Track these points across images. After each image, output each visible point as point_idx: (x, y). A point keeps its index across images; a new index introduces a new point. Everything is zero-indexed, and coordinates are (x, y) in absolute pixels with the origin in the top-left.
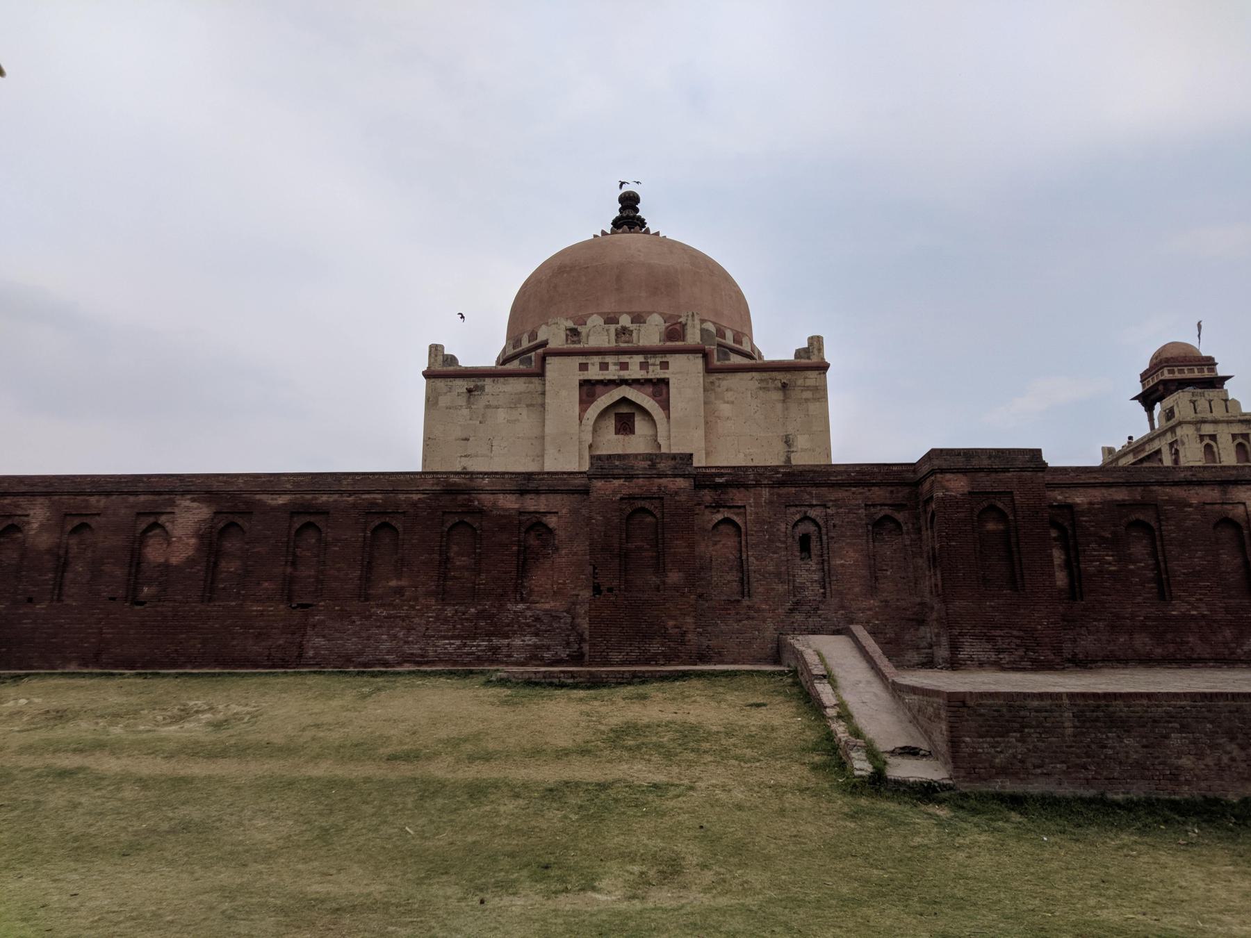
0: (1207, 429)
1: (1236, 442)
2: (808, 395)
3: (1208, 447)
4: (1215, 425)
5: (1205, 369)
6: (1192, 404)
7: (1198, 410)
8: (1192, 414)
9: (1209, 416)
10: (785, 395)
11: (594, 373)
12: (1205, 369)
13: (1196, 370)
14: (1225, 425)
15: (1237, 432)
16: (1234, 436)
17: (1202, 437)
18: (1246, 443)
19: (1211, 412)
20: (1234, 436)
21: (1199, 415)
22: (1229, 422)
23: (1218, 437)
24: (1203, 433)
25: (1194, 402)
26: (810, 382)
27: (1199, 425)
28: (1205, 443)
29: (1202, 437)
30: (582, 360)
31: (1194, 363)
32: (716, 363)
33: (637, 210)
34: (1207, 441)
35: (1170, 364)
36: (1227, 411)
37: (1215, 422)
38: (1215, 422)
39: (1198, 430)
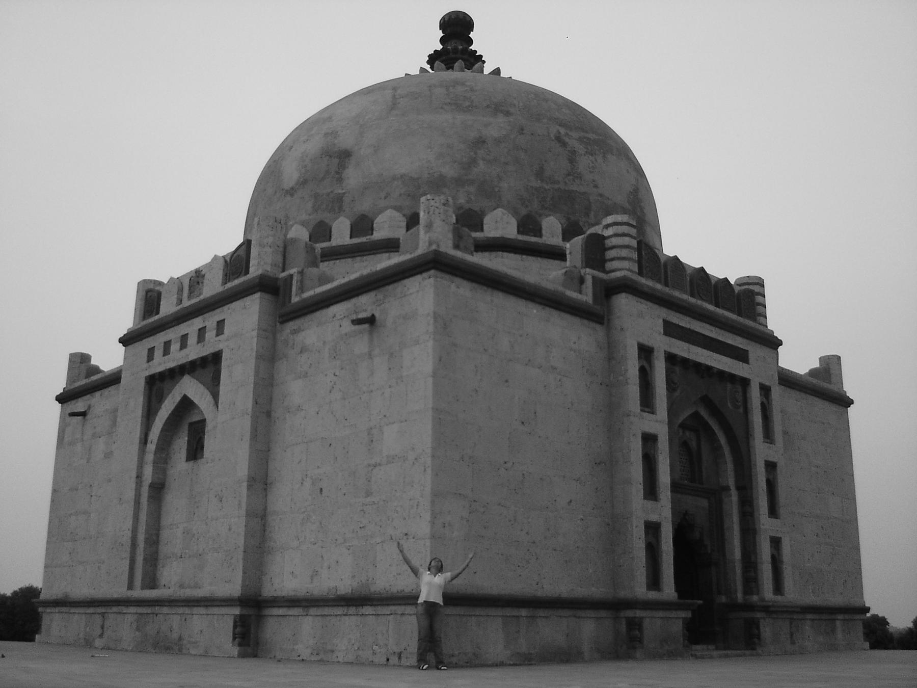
11: (160, 364)
33: (471, 42)
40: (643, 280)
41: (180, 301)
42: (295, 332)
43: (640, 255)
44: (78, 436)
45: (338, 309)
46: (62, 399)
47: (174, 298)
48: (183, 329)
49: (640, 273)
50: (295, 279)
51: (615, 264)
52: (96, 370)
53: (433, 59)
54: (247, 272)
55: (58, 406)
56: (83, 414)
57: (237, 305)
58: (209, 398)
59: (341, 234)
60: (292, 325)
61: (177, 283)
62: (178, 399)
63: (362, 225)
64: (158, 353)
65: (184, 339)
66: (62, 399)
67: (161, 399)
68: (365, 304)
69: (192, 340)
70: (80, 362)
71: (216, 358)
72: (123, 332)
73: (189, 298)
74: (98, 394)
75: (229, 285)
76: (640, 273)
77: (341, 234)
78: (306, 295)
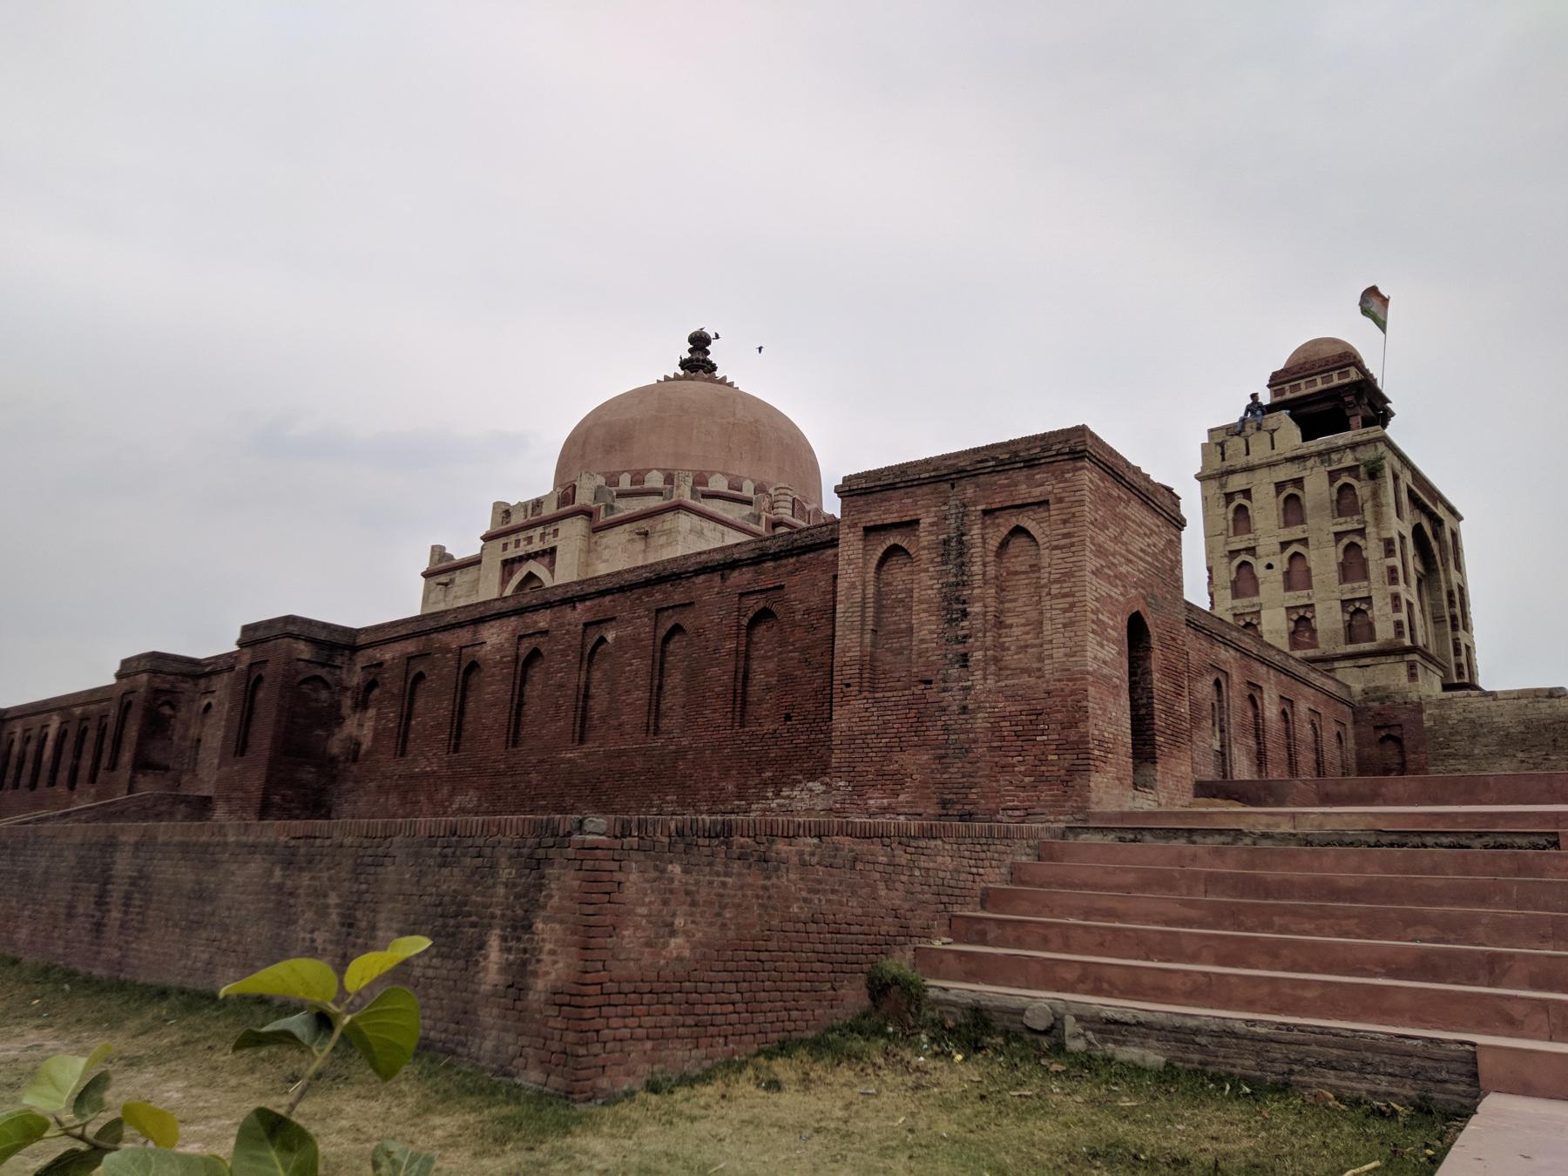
0: (1237, 483)
2: (663, 540)
4: (1250, 474)
5: (1335, 375)
6: (1219, 448)
9: (1241, 461)
10: (647, 546)
11: (512, 553)
12: (1335, 375)
14: (1265, 471)
15: (1283, 479)
16: (1280, 486)
17: (1229, 497)
19: (1248, 454)
20: (1280, 486)
21: (1227, 463)
22: (1270, 465)
23: (1253, 491)
25: (1222, 445)
26: (667, 526)
27: (1224, 478)
28: (1233, 505)
29: (1229, 497)
30: (502, 540)
31: (1313, 371)
32: (603, 518)
34: (1239, 500)
35: (1278, 381)
36: (1273, 448)
37: (1249, 469)
38: (1249, 469)
39: (1223, 486)
40: (794, 520)
41: (526, 517)
42: (601, 537)
43: (793, 505)
44: (441, 597)
45: (627, 526)
46: (426, 575)
47: (522, 514)
48: (530, 533)
49: (793, 516)
50: (602, 508)
51: (780, 510)
52: (451, 557)
53: (684, 364)
54: (573, 503)
55: (423, 580)
56: (446, 585)
57: (567, 521)
58: (547, 572)
59: (625, 483)
60: (602, 534)
61: (524, 506)
62: (525, 573)
63: (638, 478)
64: (511, 547)
65: (530, 540)
66: (426, 575)
67: (511, 574)
68: (644, 525)
69: (536, 540)
70: (439, 553)
71: (553, 550)
72: (483, 533)
73: (532, 515)
74: (458, 572)
75: (562, 510)
76: (793, 516)
77: (625, 483)
78: (609, 518)
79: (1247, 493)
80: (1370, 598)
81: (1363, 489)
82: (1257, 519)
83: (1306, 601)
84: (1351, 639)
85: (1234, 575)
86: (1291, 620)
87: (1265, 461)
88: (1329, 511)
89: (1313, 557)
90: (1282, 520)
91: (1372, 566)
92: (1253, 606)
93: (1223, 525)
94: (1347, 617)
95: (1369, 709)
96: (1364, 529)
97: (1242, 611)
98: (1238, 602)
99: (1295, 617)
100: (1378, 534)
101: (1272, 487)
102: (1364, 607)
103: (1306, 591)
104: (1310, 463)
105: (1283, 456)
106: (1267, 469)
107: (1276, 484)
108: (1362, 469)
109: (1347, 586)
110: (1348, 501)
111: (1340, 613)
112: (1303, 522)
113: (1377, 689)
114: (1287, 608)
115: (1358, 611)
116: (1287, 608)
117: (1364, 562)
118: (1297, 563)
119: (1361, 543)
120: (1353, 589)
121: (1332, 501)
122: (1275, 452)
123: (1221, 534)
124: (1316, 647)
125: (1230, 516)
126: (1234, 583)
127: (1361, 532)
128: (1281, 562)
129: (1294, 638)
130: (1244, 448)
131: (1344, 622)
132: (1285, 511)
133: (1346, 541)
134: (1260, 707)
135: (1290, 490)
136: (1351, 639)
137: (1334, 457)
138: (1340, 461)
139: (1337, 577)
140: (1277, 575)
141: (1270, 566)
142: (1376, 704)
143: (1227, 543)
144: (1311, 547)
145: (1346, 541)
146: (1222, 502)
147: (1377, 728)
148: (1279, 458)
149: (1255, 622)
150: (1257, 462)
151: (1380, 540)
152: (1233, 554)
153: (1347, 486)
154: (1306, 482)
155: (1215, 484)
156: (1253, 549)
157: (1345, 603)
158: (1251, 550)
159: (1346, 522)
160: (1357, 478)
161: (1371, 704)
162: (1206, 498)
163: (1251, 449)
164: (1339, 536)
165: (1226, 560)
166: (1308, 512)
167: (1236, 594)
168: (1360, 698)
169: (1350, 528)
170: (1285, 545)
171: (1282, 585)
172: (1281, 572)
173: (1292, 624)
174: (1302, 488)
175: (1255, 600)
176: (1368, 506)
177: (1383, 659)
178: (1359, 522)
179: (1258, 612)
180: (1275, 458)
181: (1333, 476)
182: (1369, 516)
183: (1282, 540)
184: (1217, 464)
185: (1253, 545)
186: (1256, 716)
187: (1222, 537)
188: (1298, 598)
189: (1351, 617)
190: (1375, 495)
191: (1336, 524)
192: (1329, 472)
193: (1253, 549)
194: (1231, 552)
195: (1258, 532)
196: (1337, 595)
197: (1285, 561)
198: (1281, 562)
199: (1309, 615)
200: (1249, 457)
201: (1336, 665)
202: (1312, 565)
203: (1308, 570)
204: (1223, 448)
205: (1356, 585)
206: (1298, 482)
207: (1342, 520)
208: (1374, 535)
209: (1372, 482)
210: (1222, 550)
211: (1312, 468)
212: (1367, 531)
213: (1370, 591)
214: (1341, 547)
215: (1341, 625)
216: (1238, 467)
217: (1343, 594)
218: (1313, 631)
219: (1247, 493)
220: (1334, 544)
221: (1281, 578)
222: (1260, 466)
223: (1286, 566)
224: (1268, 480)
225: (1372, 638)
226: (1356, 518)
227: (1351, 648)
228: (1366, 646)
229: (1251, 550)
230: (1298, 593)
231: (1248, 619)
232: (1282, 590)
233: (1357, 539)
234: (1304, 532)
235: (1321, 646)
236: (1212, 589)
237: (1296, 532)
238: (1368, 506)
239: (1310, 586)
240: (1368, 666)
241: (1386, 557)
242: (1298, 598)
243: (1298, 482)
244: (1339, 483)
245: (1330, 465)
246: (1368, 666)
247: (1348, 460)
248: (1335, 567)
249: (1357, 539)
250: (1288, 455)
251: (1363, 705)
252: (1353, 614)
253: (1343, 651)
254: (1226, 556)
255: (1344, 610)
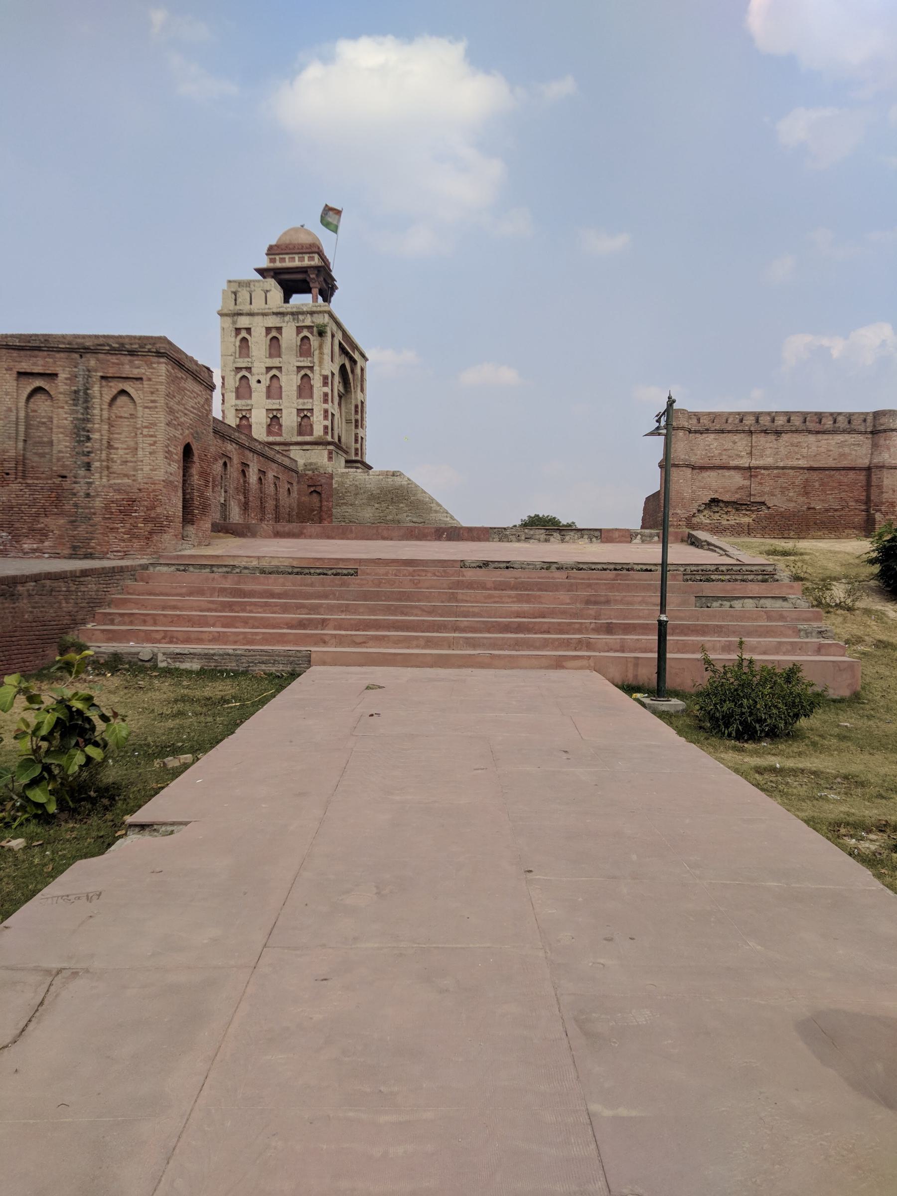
0: (243, 322)
1: (240, 337)
3: (244, 339)
4: (251, 318)
6: (233, 296)
7: (238, 302)
8: (263, 305)
9: (246, 308)
13: (297, 259)
14: (260, 317)
15: (270, 325)
16: (268, 330)
17: (238, 331)
18: (279, 336)
19: (251, 303)
20: (268, 330)
22: (264, 315)
23: (252, 330)
24: (238, 327)
25: (235, 293)
27: (235, 318)
28: (240, 337)
29: (238, 331)
34: (244, 334)
36: (266, 303)
37: (251, 314)
38: (251, 314)
39: (234, 323)
79: (248, 330)
80: (312, 409)
81: (314, 341)
82: (253, 349)
83: (277, 407)
84: (300, 433)
85: (238, 383)
86: (269, 417)
87: (260, 311)
88: (295, 352)
89: (284, 379)
90: (268, 352)
91: (315, 390)
92: (248, 405)
93: (233, 350)
94: (299, 419)
95: (307, 475)
96: (313, 367)
97: (241, 408)
98: (239, 402)
99: (271, 416)
100: (320, 371)
101: (264, 330)
102: (309, 414)
103: (278, 401)
104: (287, 318)
105: (271, 311)
106: (262, 316)
107: (266, 328)
108: (315, 329)
109: (301, 401)
110: (306, 347)
111: (296, 416)
112: (280, 356)
113: (311, 464)
114: (267, 410)
115: (306, 416)
116: (267, 410)
117: (311, 387)
118: (275, 380)
119: (311, 375)
120: (304, 403)
121: (297, 345)
122: (267, 306)
123: (232, 355)
124: (281, 435)
125: (238, 344)
126: (237, 389)
127: (311, 368)
128: (266, 379)
129: (269, 429)
130: (249, 299)
131: (298, 422)
132: (270, 346)
133: (303, 373)
134: (247, 476)
135: (274, 333)
136: (300, 433)
137: (301, 317)
138: (303, 321)
139: (296, 395)
140: (262, 388)
141: (259, 382)
142: (310, 473)
143: (234, 362)
144: (283, 373)
145: (303, 373)
146: (233, 334)
147: (309, 486)
148: (269, 311)
149: (248, 416)
150: (256, 311)
151: (321, 375)
152: (238, 369)
153: (306, 337)
154: (284, 330)
155: (229, 320)
156: (250, 368)
157: (299, 411)
158: (249, 369)
159: (304, 361)
160: (312, 333)
161: (307, 472)
162: (224, 329)
163: (253, 300)
164: (299, 368)
165: (233, 373)
166: (283, 350)
167: (238, 397)
168: (302, 468)
169: (306, 365)
170: (269, 369)
171: (265, 394)
172: (265, 386)
173: (269, 420)
174: (281, 334)
175: (249, 402)
176: (317, 353)
177: (316, 447)
178: (310, 362)
179: (251, 410)
180: (266, 311)
181: (299, 329)
182: (316, 360)
183: (267, 366)
184: (231, 307)
185: (250, 366)
186: (245, 482)
187: (233, 357)
188: (273, 404)
189: (301, 420)
190: (321, 347)
191: (298, 361)
192: (297, 327)
193: (250, 368)
194: (236, 368)
195: (254, 358)
196: (295, 405)
197: (268, 379)
198: (266, 380)
199: (279, 416)
200: (252, 307)
201: (292, 447)
202: (283, 384)
203: (281, 387)
204: (236, 295)
205: (306, 401)
206: (279, 329)
207: (302, 359)
208: (318, 372)
209: (320, 338)
210: (232, 366)
211: (287, 322)
212: (315, 368)
213: (313, 405)
214: (300, 376)
215: (296, 424)
216: (244, 312)
217: (298, 405)
218: (281, 426)
219: (248, 330)
220: (296, 373)
221: (264, 390)
222: (258, 314)
223: (268, 383)
224: (262, 325)
225: (311, 434)
226: (309, 359)
227: (300, 439)
228: (308, 438)
229: (249, 369)
230: (273, 401)
231: (244, 414)
232: (265, 398)
233: (309, 372)
234: (280, 363)
235: (284, 435)
236: (224, 392)
237: (275, 362)
238: (317, 353)
239: (281, 398)
240: (308, 450)
241: (323, 386)
242: (273, 404)
243: (279, 329)
244: (302, 335)
245: (298, 322)
246: (308, 450)
247: (308, 322)
248: (295, 388)
249: (309, 372)
250: (275, 310)
251: (303, 472)
252: (302, 418)
253: (296, 440)
254: (233, 370)
255: (298, 415)
